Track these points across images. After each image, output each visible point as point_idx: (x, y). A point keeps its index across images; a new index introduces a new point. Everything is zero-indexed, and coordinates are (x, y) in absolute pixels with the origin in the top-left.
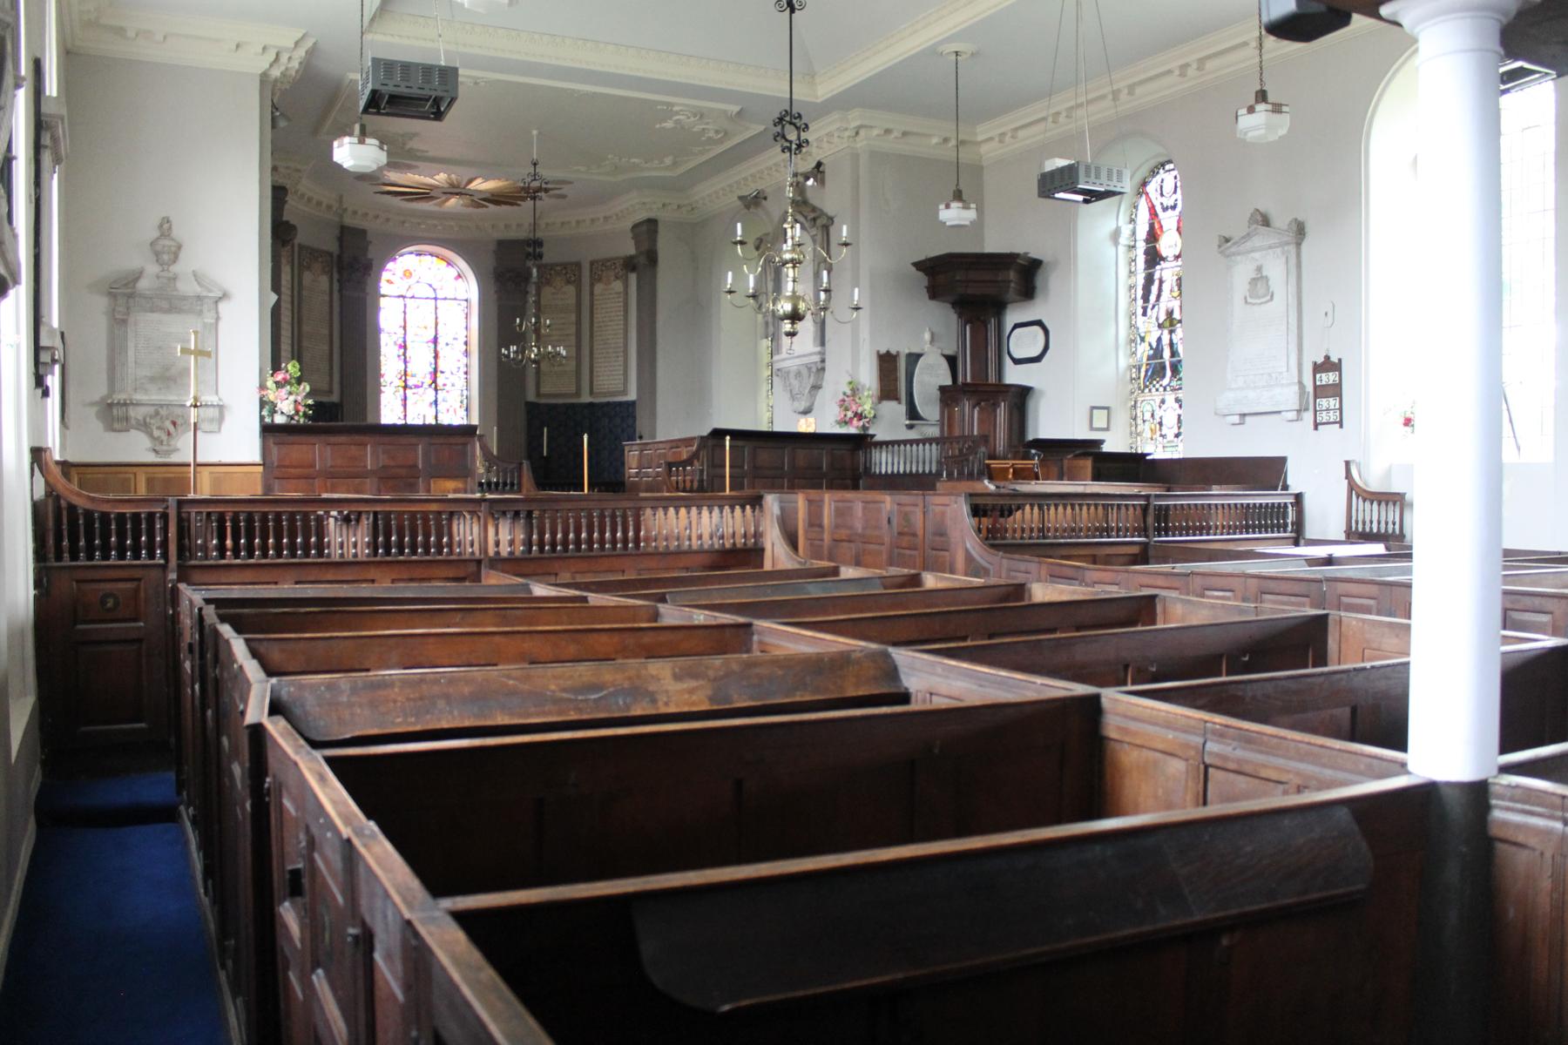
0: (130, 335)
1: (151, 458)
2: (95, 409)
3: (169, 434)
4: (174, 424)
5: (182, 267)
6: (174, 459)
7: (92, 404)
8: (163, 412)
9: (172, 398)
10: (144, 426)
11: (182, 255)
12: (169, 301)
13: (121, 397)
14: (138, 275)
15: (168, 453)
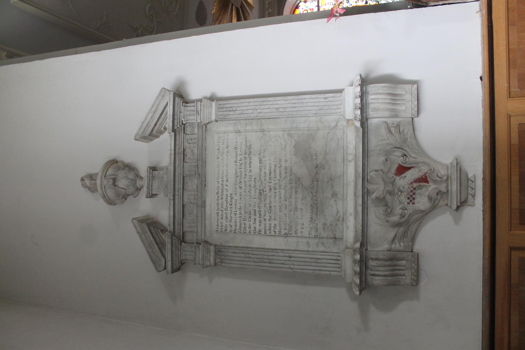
0: (240, 241)
1: (475, 214)
2: (376, 316)
3: (424, 179)
4: (402, 170)
5: (141, 155)
6: (476, 167)
7: (364, 313)
8: (378, 189)
9: (351, 171)
10: (408, 226)
11: (127, 160)
12: (186, 174)
13: (349, 266)
14: (150, 226)
15: (464, 180)
